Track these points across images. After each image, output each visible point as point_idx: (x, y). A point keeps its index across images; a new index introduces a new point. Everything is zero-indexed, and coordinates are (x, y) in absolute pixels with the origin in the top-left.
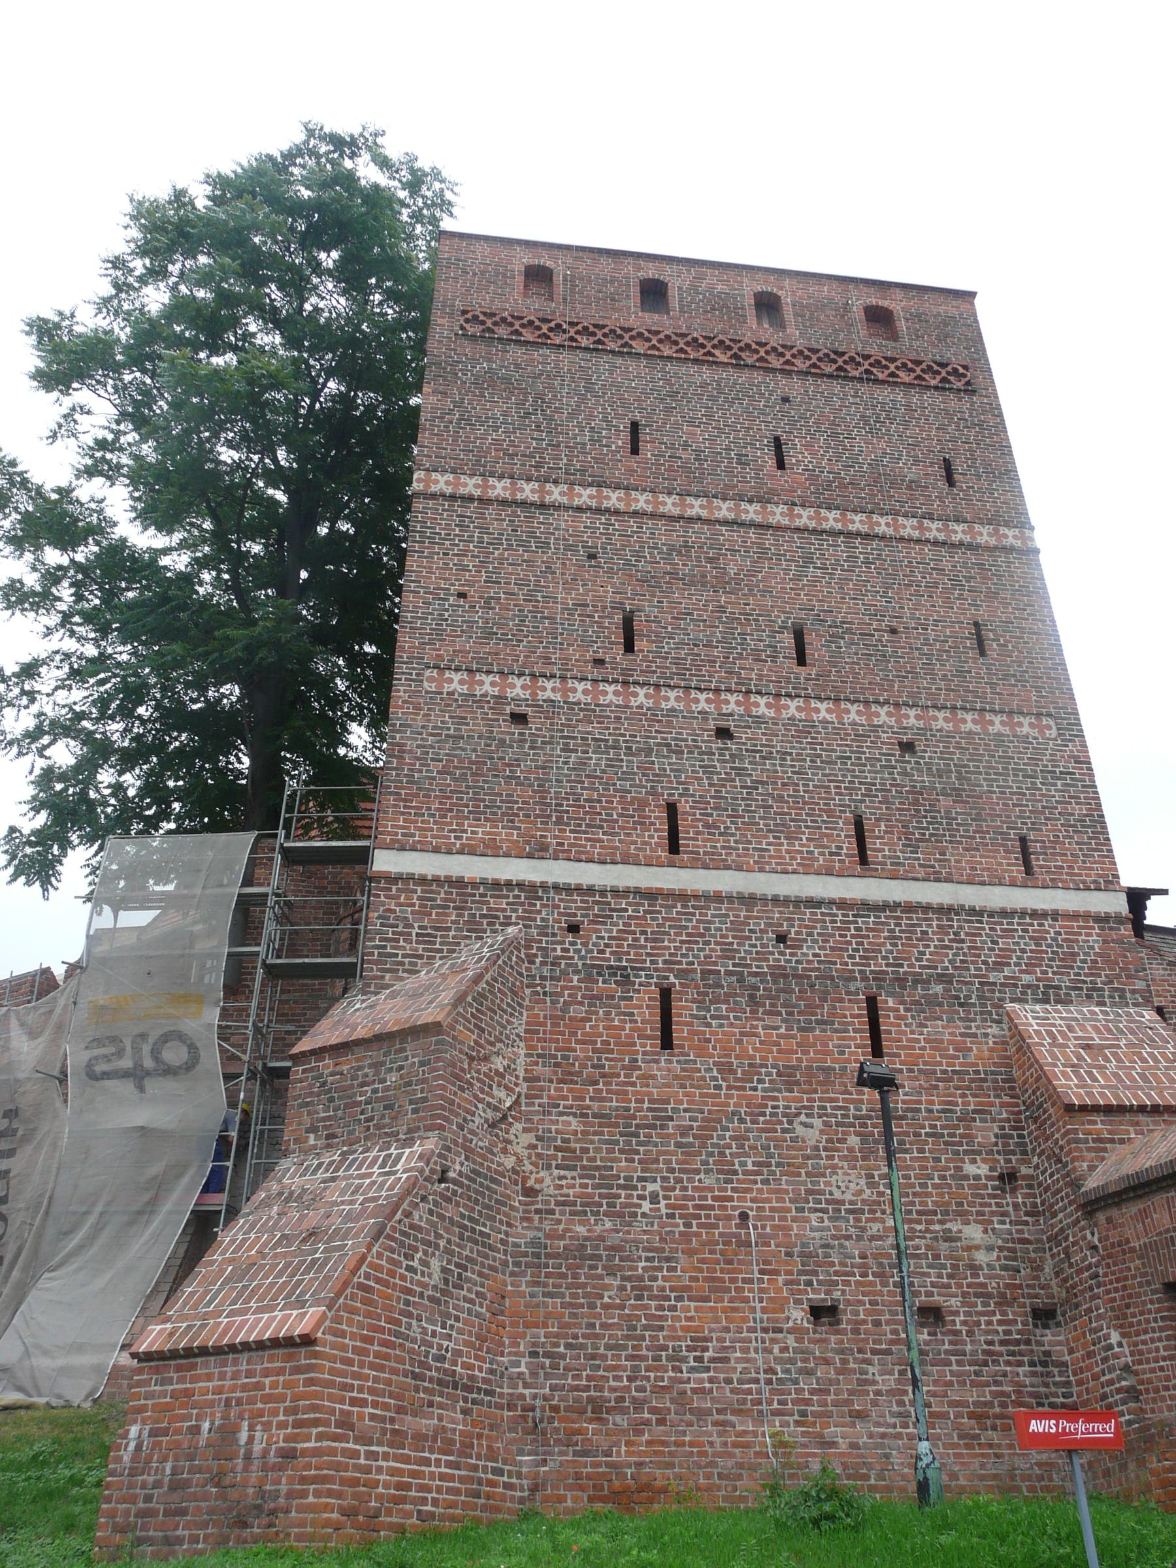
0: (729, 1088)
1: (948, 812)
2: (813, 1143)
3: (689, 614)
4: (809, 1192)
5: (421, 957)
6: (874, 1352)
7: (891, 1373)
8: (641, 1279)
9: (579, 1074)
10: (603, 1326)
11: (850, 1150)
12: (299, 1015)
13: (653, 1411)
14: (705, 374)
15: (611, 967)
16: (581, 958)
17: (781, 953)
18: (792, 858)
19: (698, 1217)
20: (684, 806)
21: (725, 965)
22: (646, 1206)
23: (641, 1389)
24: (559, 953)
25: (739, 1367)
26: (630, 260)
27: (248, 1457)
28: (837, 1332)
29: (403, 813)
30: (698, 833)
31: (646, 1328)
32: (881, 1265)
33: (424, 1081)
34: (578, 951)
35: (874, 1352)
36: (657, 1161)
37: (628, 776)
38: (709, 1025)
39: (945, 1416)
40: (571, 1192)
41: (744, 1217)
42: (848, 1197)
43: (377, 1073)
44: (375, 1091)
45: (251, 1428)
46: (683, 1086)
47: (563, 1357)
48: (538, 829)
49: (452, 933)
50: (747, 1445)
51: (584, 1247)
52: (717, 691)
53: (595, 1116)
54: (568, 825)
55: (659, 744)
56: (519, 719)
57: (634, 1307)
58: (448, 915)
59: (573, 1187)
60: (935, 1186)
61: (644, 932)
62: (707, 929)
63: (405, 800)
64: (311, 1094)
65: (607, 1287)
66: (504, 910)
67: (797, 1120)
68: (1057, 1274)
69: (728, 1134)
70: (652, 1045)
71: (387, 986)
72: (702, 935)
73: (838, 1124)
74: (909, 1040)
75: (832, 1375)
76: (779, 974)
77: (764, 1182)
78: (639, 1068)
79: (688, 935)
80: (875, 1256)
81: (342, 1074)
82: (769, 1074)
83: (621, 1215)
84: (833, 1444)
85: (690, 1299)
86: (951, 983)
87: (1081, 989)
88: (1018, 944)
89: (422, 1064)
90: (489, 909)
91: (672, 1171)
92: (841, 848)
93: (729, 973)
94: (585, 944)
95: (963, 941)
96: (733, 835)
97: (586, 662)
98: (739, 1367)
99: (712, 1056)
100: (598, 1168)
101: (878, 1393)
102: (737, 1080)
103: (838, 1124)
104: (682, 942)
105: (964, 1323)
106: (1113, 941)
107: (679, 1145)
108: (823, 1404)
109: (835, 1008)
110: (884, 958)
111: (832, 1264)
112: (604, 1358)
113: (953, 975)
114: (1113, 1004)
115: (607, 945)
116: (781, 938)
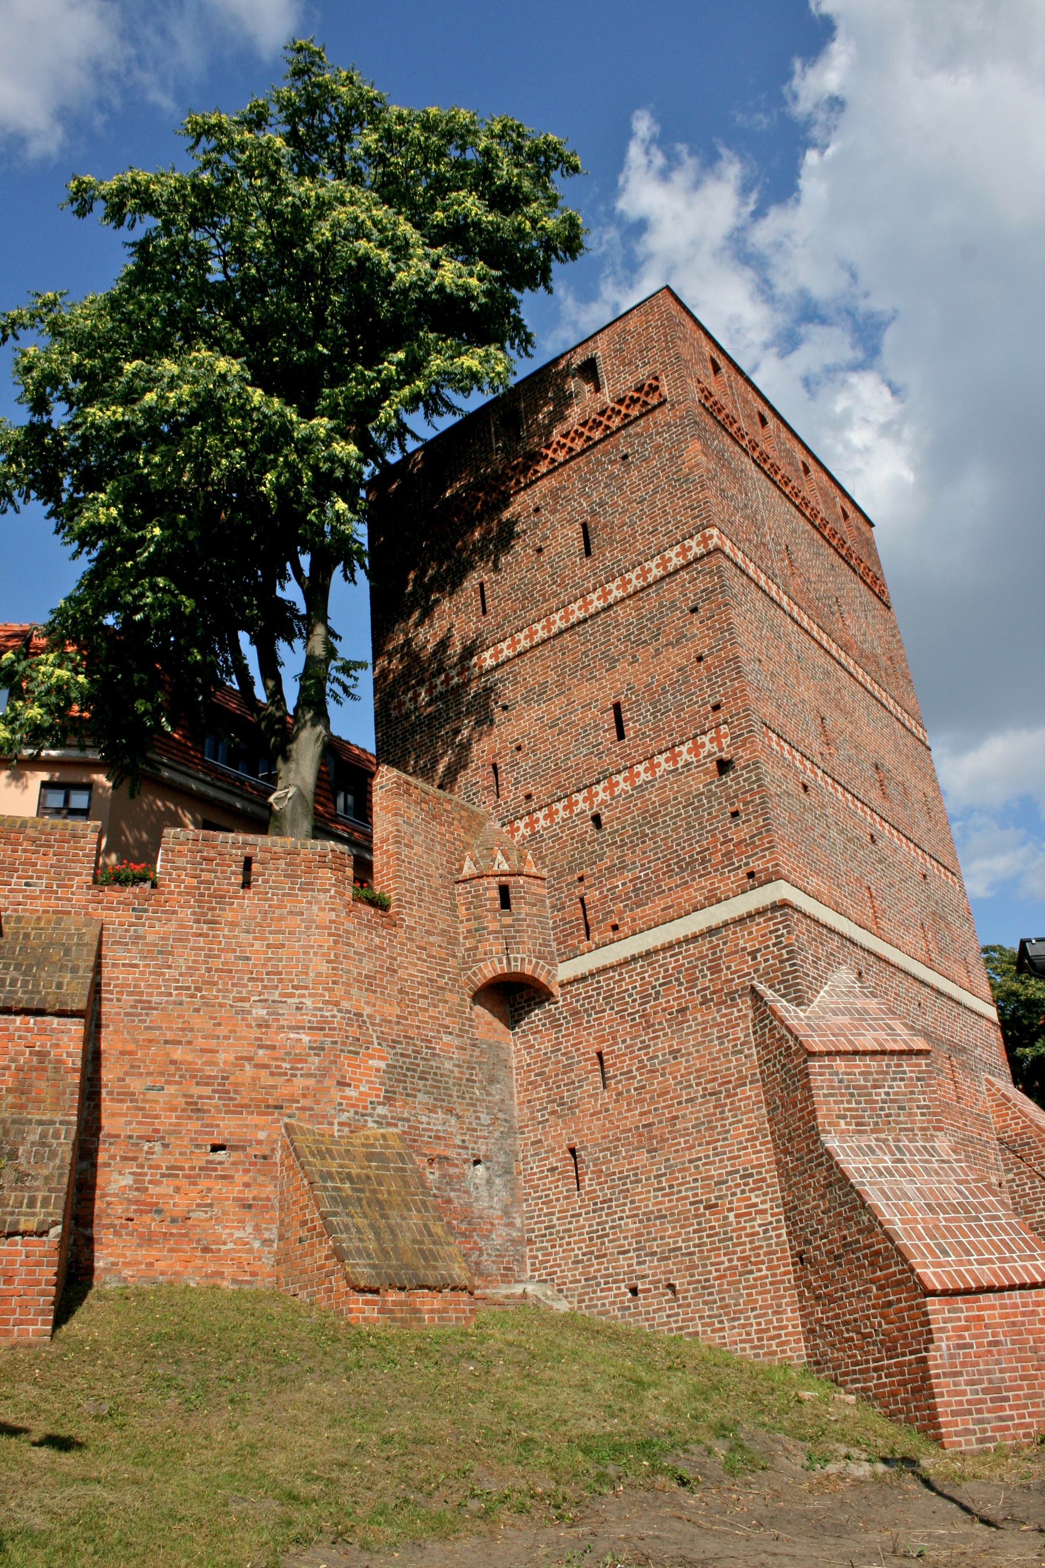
33: (924, 1093)
71: (811, 1001)
89: (918, 1079)
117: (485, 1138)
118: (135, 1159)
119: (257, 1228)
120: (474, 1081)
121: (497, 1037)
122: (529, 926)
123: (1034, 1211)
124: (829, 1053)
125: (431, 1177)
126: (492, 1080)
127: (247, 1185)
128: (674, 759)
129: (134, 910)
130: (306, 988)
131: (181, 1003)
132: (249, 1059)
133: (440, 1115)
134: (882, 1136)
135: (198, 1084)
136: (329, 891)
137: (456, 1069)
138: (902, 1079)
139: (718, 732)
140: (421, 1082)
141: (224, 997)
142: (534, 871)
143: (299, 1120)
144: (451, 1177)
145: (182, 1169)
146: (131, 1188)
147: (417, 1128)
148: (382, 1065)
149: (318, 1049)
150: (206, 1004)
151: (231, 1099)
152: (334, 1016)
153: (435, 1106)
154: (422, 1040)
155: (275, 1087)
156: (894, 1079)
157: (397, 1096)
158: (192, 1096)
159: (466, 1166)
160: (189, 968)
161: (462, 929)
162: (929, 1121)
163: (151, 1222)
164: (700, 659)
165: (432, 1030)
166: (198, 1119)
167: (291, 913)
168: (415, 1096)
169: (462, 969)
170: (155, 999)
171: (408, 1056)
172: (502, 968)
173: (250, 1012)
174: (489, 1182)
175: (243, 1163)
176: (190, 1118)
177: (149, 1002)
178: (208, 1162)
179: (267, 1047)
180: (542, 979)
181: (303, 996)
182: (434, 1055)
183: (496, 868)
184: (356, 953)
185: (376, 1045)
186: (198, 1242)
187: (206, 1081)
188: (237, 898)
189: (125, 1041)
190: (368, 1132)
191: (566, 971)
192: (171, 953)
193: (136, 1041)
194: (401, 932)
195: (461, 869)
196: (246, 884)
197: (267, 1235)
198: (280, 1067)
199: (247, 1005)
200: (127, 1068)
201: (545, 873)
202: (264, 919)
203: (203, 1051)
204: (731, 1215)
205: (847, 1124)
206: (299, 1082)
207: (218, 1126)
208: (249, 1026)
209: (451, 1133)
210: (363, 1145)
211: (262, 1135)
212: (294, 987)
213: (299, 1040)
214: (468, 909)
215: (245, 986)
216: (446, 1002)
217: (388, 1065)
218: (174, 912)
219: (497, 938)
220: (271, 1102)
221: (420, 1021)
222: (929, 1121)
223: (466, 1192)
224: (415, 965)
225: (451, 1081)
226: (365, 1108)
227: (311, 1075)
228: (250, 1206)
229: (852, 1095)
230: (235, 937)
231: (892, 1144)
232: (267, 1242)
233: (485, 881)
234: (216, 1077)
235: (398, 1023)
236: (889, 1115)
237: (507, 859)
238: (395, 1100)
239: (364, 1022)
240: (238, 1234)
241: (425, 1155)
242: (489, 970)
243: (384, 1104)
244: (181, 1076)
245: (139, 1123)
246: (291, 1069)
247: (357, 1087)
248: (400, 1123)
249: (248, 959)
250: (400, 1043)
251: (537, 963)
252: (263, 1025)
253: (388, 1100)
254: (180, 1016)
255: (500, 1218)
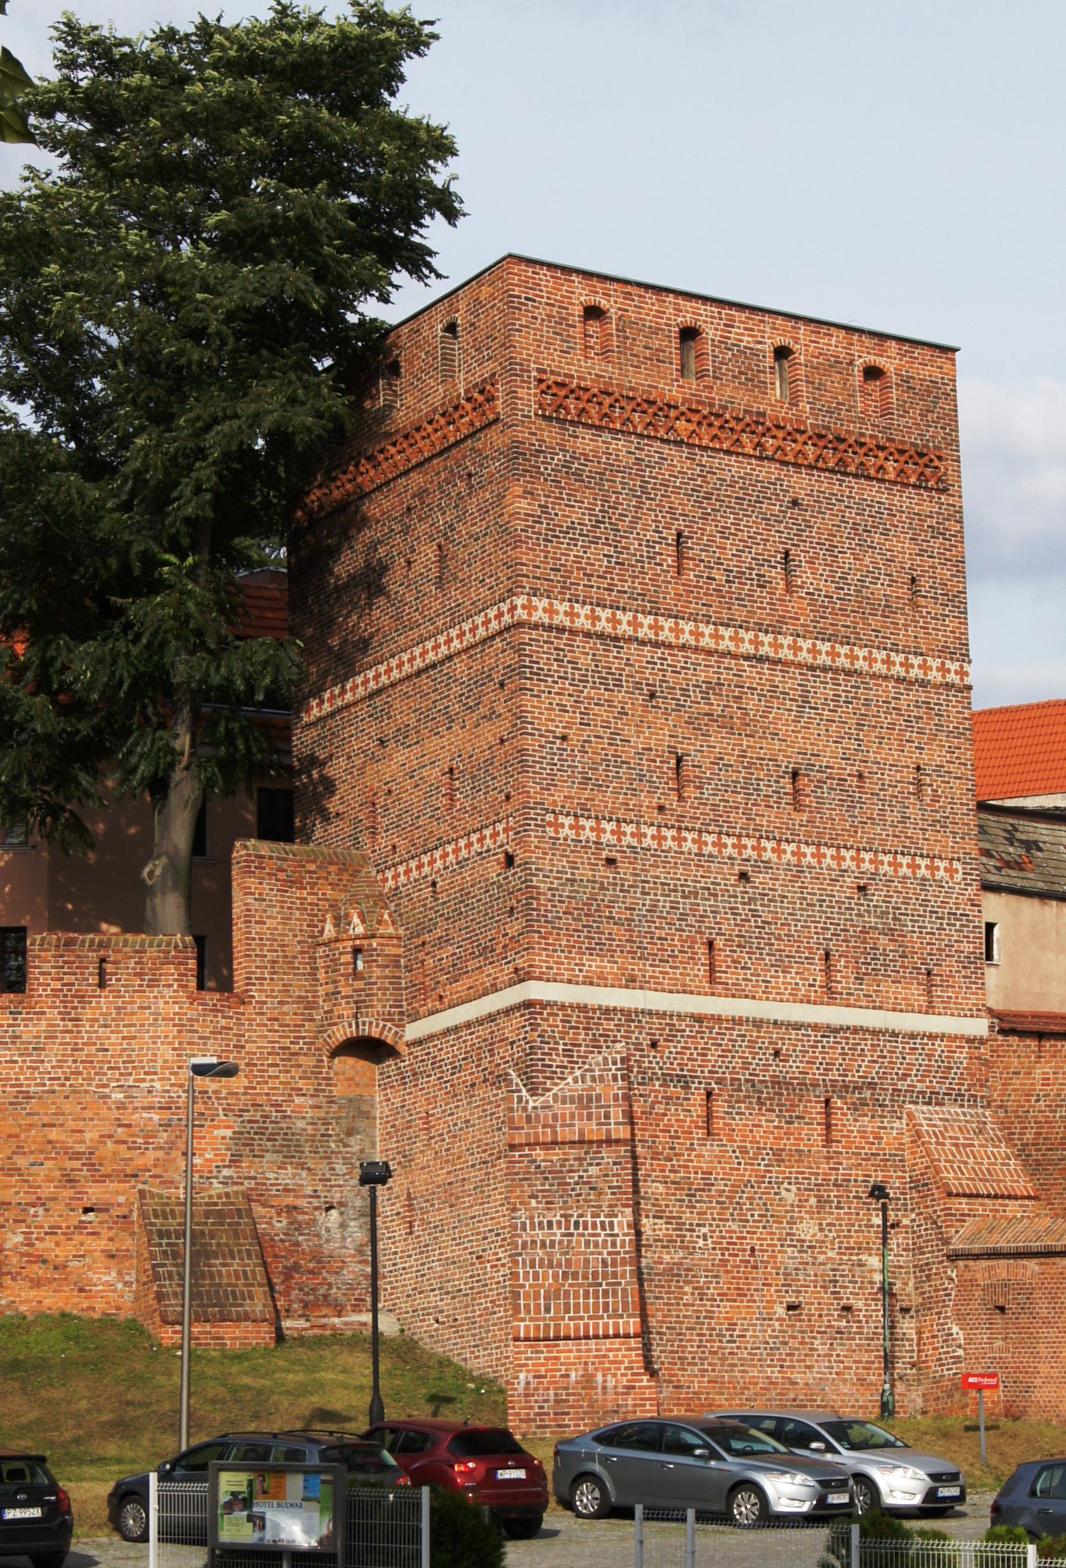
0: (746, 1164)
1: (885, 950)
2: (790, 1202)
3: (722, 759)
4: (788, 1234)
5: (566, 1067)
6: (819, 1332)
7: (825, 1344)
8: (702, 1288)
9: (662, 1153)
10: (685, 1317)
11: (811, 1207)
12: (300, 1026)
13: (709, 1364)
14: (733, 467)
15: (677, 1076)
16: (661, 1068)
17: (777, 1066)
18: (786, 989)
19: (728, 1249)
20: (719, 942)
21: (744, 1075)
22: (701, 1242)
23: (703, 1352)
24: (646, 1064)
25: (752, 1340)
26: (671, 298)
27: (604, 1388)
28: (800, 1321)
29: (545, 950)
30: (728, 967)
31: (705, 1317)
32: (824, 1281)
33: (618, 1175)
34: (658, 1063)
35: (819, 1332)
36: (705, 1213)
37: (683, 917)
38: (734, 1119)
39: (850, 1368)
40: (660, 1233)
41: (753, 1249)
42: (808, 1238)
43: (581, 1165)
44: (581, 1177)
45: (604, 1375)
46: (720, 1162)
47: (665, 1334)
48: (630, 964)
49: (583, 1049)
50: (756, 1383)
51: (672, 1269)
52: (740, 836)
53: (673, 1183)
54: (647, 960)
55: (703, 888)
56: (610, 862)
57: (699, 1305)
58: (579, 1034)
59: (661, 1230)
60: (856, 1231)
61: (696, 1049)
62: (734, 1046)
63: (545, 938)
64: (529, 1173)
65: (685, 1293)
66: (612, 1031)
67: (782, 1186)
68: (917, 1289)
69: (745, 1195)
70: (701, 1133)
71: (549, 1090)
72: (730, 1051)
73: (806, 1190)
74: (849, 1131)
75: (797, 1346)
76: (776, 1082)
77: (764, 1227)
78: (695, 1150)
79: (723, 1051)
80: (822, 1275)
81: (552, 1161)
82: (768, 1154)
83: (687, 1248)
84: (797, 1383)
85: (728, 1300)
86: (875, 1089)
87: (950, 1095)
88: (917, 1059)
89: (615, 1163)
90: (604, 1030)
91: (714, 1219)
92: (815, 980)
93: (747, 1081)
94: (662, 1057)
95: (885, 1057)
96: (749, 969)
97: (653, 808)
98: (752, 1340)
99: (735, 1141)
100: (674, 1218)
101: (819, 1356)
102: (750, 1158)
103: (806, 1190)
104: (719, 1056)
105: (865, 1316)
106: (976, 1058)
107: (718, 1202)
108: (792, 1361)
109: (806, 1107)
110: (838, 1070)
111: (799, 1280)
112: (685, 1335)
113: (876, 1084)
114: (969, 1106)
115: (675, 1059)
116: (777, 1053)
117: (340, 1186)
118: (24, 1221)
119: (120, 1273)
120: (330, 1136)
121: (358, 1091)
122: (379, 989)
123: (924, 1253)
124: (528, 1144)
125: (278, 1225)
126: (350, 1132)
127: (111, 1239)
128: (481, 840)
129: (11, 1013)
130: (155, 1073)
131: (54, 1092)
132: (110, 1136)
133: (290, 1170)
134: (570, 1212)
135: (70, 1159)
136: (171, 986)
137: (309, 1127)
138: (598, 1164)
139: (508, 823)
140: (270, 1144)
141: (89, 1085)
142: (391, 930)
143: (152, 1186)
144: (299, 1223)
145: (60, 1228)
146: (23, 1245)
147: (265, 1184)
148: (229, 1133)
149: (166, 1125)
150: (74, 1092)
151: (96, 1170)
152: (179, 1097)
153: (284, 1163)
154: (272, 1106)
155: (131, 1159)
156: (591, 1164)
157: (244, 1159)
158: (65, 1169)
159: (317, 1213)
160: (58, 1061)
161: (321, 991)
162: (618, 1200)
163: (39, 1270)
164: (502, 741)
165: (283, 1095)
166: (71, 1188)
167: (140, 1008)
168: (262, 1157)
169: (320, 1032)
170: (32, 1089)
171: (257, 1122)
172: (351, 1032)
173: (109, 1097)
174: (343, 1226)
175: (107, 1222)
176: (65, 1187)
177: (28, 1092)
178: (81, 1222)
179: (125, 1126)
180: (389, 1041)
181: (153, 1080)
182: (285, 1117)
183: (351, 932)
184: (200, 1038)
185: (222, 1117)
186: (75, 1284)
187: (76, 1156)
188: (94, 997)
189: (11, 1126)
190: (213, 1193)
191: (413, 1031)
192: (43, 1049)
193: (20, 1125)
194: (250, 1010)
195: (322, 932)
196: (102, 984)
197: (127, 1278)
198: (135, 1142)
199: (107, 1090)
200: (14, 1149)
201: (401, 931)
202: (118, 1014)
203: (74, 1131)
204: (488, 1265)
205: (538, 1202)
206: (152, 1155)
207: (87, 1193)
208: (109, 1109)
209: (302, 1185)
210: (207, 1204)
211: (122, 1199)
212: (146, 1073)
213: (151, 1119)
214: (327, 972)
215: (105, 1074)
216: (300, 1066)
217: (234, 1133)
218: (44, 1013)
219: (348, 1003)
220: (129, 1172)
221: (270, 1089)
222: (618, 1200)
223: (318, 1236)
224: (266, 1036)
225: (303, 1139)
226: (210, 1172)
227: (161, 1148)
228: (113, 1256)
229: (546, 1179)
230: (96, 1032)
231: (573, 1220)
232: (126, 1284)
233: (340, 945)
234: (84, 1153)
235: (245, 1094)
236: (580, 1195)
237: (363, 921)
238: (241, 1162)
239: (210, 1098)
240: (105, 1278)
241: (273, 1207)
242: (341, 1033)
243: (230, 1167)
244: (57, 1153)
245: (25, 1193)
246: (145, 1143)
247: (202, 1155)
248: (246, 1182)
249: (107, 1050)
250: (248, 1111)
251: (385, 1026)
252: (121, 1106)
253: (235, 1161)
254: (53, 1103)
255: (354, 1256)
